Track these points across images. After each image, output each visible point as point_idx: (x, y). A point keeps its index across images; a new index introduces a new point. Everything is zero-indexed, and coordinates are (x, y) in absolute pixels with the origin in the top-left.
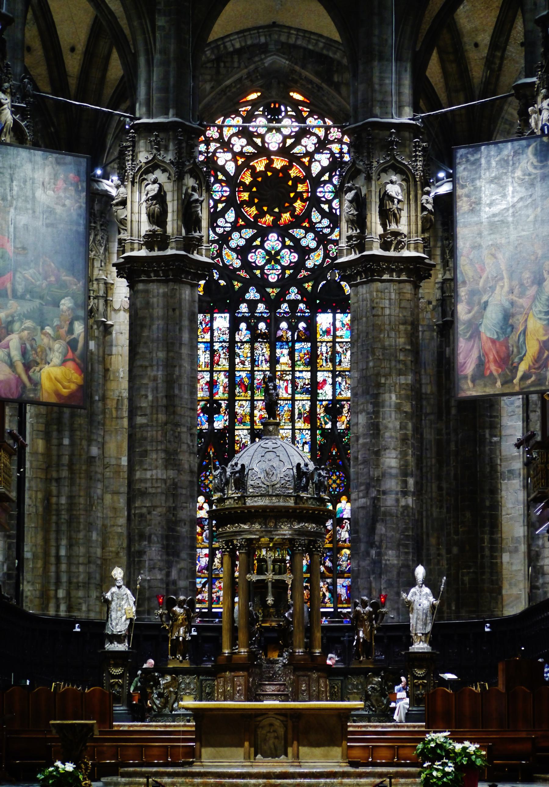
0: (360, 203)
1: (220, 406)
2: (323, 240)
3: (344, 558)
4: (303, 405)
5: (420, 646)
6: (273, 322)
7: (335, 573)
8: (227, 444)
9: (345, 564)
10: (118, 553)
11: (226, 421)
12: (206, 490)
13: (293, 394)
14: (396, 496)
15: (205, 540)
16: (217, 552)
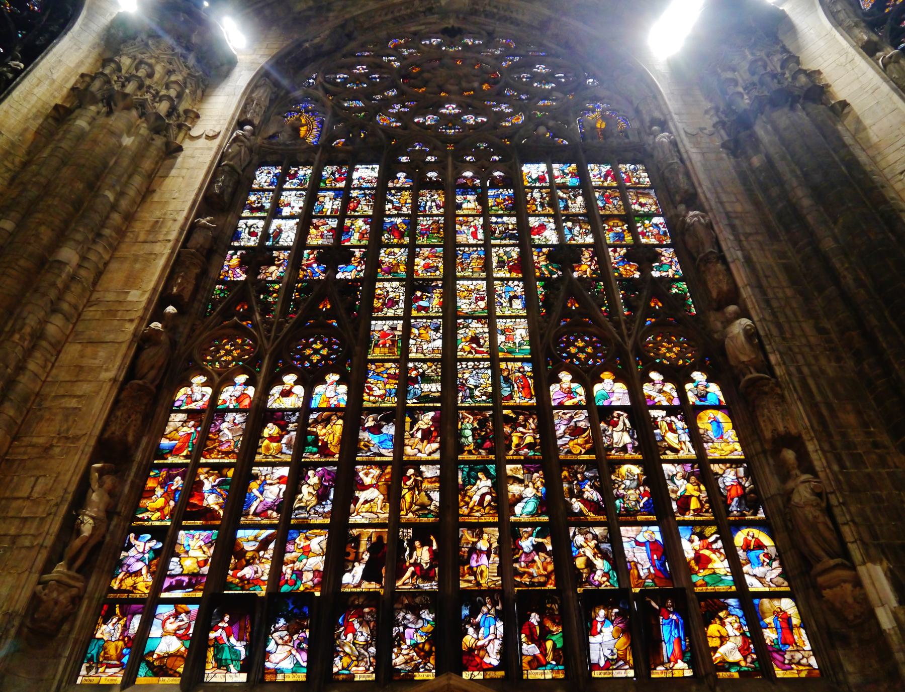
1: (352, 254)
3: (628, 483)
4: (506, 253)
8: (358, 299)
9: (632, 495)
10: (48, 448)
11: (361, 271)
12: (303, 364)
13: (487, 239)
15: (285, 450)
16: (311, 473)
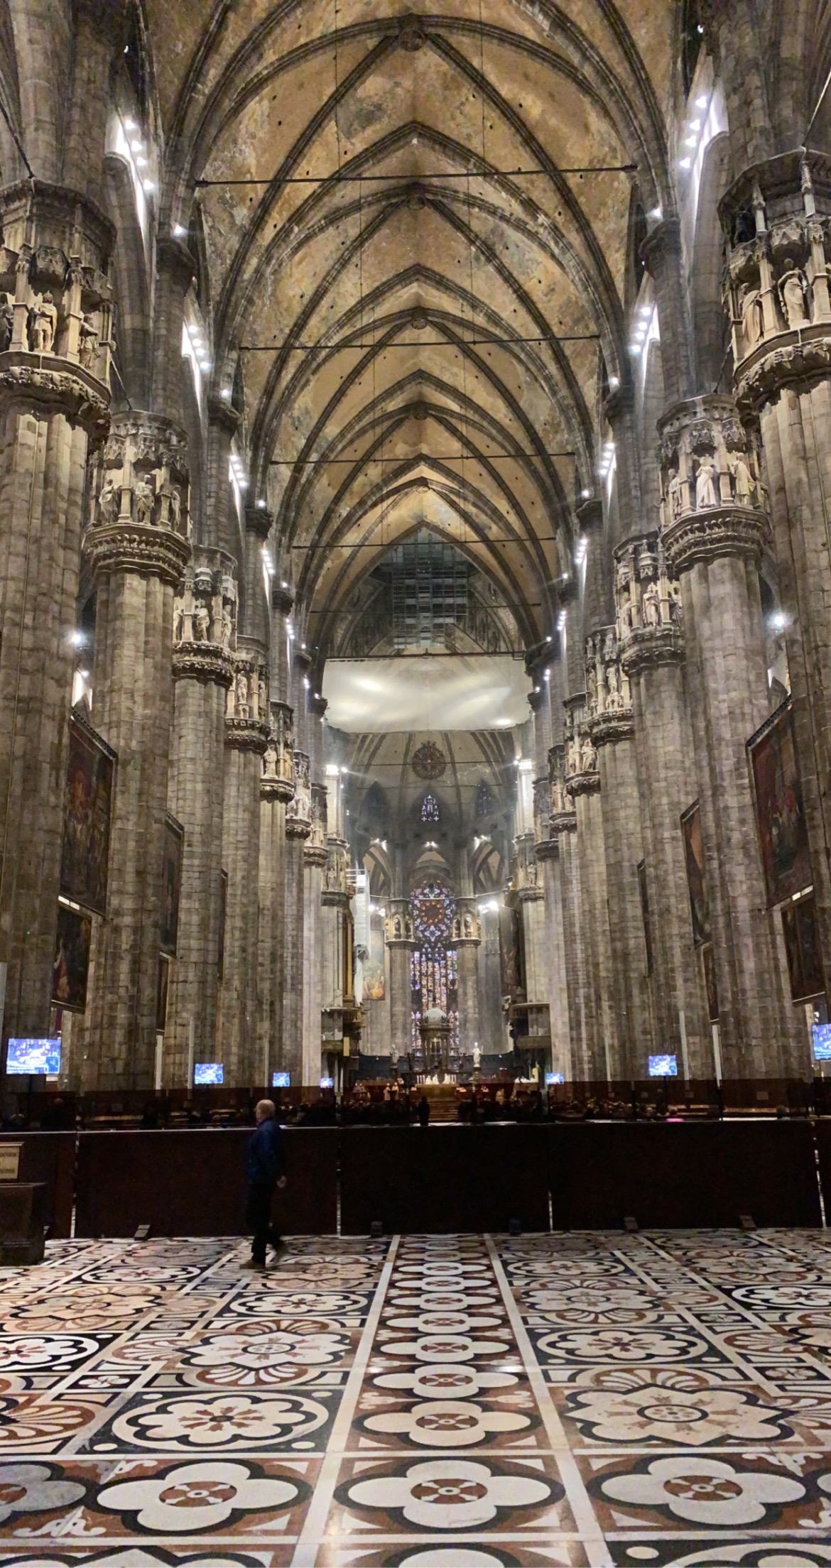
0: (458, 923)
2: (448, 927)
5: (477, 1065)
6: (433, 954)
7: (456, 1036)
14: (472, 1014)
